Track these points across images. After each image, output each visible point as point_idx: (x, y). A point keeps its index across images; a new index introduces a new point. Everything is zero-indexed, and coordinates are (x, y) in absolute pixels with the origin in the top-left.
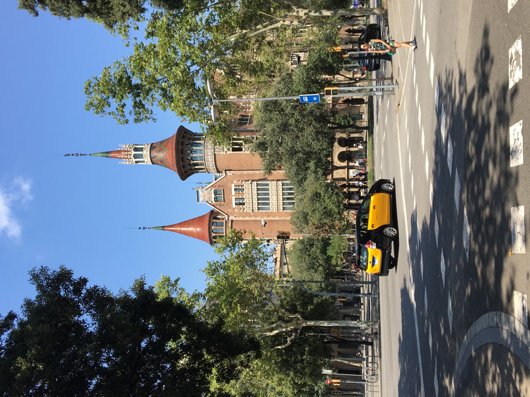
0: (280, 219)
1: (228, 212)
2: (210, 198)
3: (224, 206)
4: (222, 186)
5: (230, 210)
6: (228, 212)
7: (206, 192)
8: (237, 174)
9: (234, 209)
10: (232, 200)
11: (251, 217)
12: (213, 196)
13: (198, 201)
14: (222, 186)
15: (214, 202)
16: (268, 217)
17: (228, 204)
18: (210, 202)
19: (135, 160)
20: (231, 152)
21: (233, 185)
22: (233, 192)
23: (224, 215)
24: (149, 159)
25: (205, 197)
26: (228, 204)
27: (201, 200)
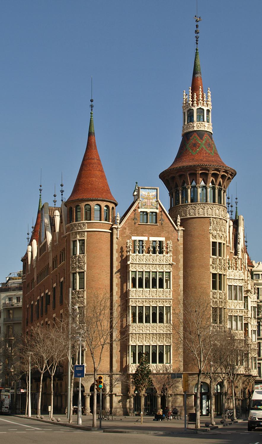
2: (145, 205)
3: (133, 224)
4: (162, 224)
6: (125, 229)
7: (154, 201)
8: (179, 245)
9: (131, 238)
10: (142, 236)
12: (149, 210)
14: (162, 224)
15: (140, 210)
17: (137, 230)
20: (212, 240)
21: (162, 239)
22: (152, 239)
23: (120, 223)
25: (147, 198)
26: (137, 230)
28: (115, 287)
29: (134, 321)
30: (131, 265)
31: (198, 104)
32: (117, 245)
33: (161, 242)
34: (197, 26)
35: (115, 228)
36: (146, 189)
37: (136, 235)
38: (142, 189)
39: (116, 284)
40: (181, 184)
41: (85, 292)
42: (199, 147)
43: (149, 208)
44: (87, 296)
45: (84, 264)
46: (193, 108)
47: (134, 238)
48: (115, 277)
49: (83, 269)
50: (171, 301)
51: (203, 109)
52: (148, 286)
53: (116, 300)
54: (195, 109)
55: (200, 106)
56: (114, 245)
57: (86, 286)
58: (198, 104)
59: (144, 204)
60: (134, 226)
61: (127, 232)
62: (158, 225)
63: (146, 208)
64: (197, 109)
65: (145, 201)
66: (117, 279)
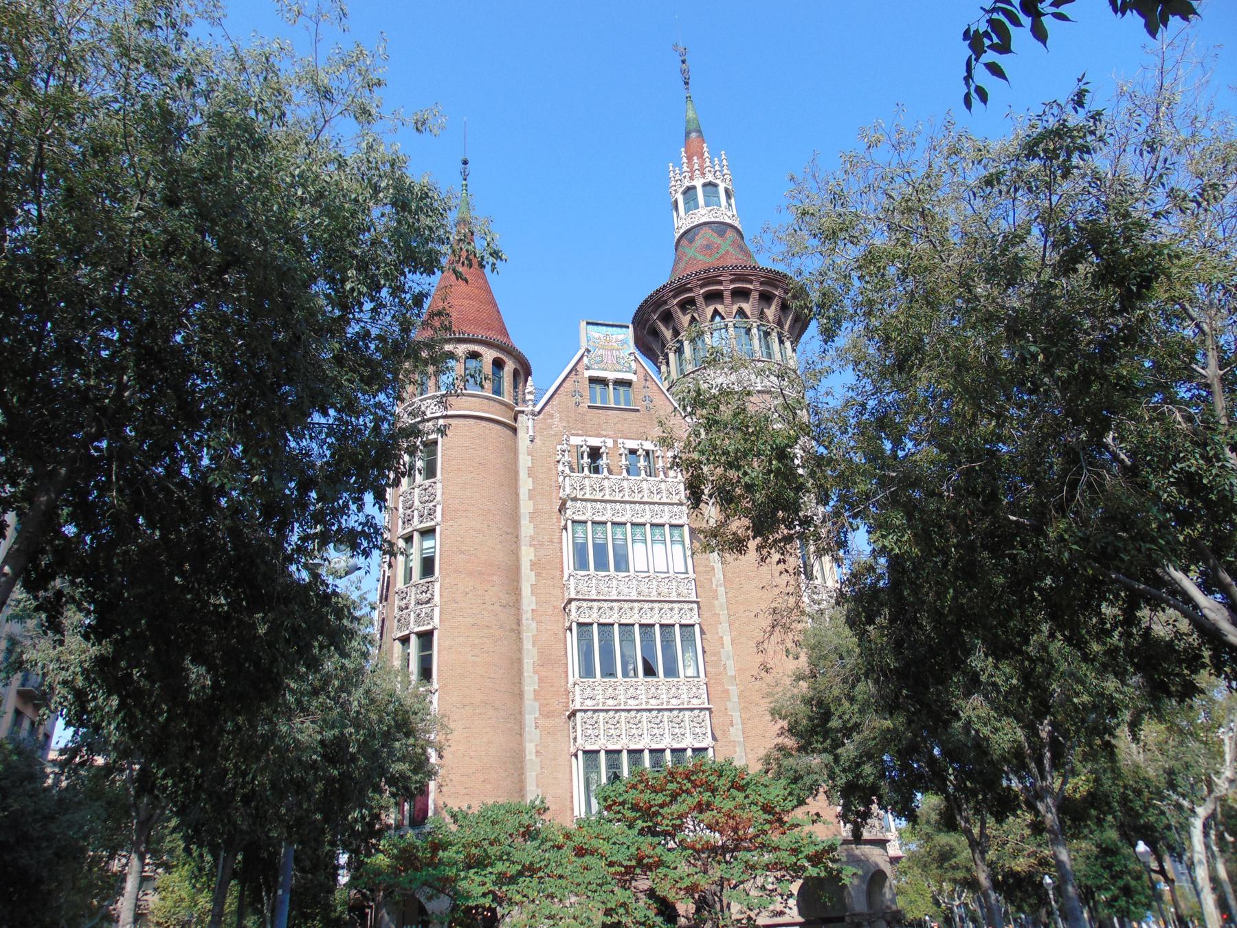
0: (526, 617)
1: (551, 416)
3: (572, 405)
5: (557, 423)
6: (551, 416)
11: (530, 498)
12: (611, 376)
13: (588, 323)
15: (588, 374)
16: (533, 565)
17: (583, 421)
18: (585, 360)
19: (698, 183)
24: (708, 220)
26: (583, 421)
27: (596, 332)
28: (528, 571)
29: (588, 671)
30: (569, 504)
31: (703, 174)
32: (530, 458)
33: (651, 453)
34: (683, 62)
35: (523, 412)
36: (600, 327)
37: (580, 432)
38: (590, 326)
39: (529, 565)
40: (686, 325)
41: (437, 585)
42: (718, 248)
43: (610, 370)
44: (441, 596)
45: (435, 506)
46: (694, 183)
47: (575, 440)
48: (528, 543)
49: (432, 519)
50: (695, 606)
51: (716, 186)
52: (623, 566)
53: (533, 610)
54: (698, 183)
55: (710, 178)
56: (521, 457)
57: (440, 568)
58: (703, 174)
59: (598, 359)
60: (575, 411)
61: (557, 423)
62: (638, 410)
63: (603, 369)
64: (704, 185)
65: (600, 352)
66: (532, 549)
